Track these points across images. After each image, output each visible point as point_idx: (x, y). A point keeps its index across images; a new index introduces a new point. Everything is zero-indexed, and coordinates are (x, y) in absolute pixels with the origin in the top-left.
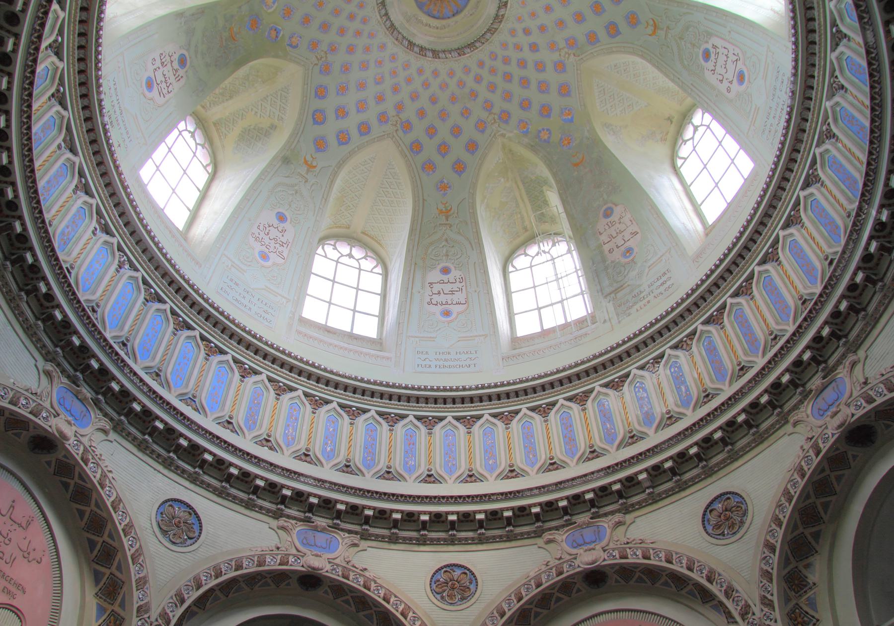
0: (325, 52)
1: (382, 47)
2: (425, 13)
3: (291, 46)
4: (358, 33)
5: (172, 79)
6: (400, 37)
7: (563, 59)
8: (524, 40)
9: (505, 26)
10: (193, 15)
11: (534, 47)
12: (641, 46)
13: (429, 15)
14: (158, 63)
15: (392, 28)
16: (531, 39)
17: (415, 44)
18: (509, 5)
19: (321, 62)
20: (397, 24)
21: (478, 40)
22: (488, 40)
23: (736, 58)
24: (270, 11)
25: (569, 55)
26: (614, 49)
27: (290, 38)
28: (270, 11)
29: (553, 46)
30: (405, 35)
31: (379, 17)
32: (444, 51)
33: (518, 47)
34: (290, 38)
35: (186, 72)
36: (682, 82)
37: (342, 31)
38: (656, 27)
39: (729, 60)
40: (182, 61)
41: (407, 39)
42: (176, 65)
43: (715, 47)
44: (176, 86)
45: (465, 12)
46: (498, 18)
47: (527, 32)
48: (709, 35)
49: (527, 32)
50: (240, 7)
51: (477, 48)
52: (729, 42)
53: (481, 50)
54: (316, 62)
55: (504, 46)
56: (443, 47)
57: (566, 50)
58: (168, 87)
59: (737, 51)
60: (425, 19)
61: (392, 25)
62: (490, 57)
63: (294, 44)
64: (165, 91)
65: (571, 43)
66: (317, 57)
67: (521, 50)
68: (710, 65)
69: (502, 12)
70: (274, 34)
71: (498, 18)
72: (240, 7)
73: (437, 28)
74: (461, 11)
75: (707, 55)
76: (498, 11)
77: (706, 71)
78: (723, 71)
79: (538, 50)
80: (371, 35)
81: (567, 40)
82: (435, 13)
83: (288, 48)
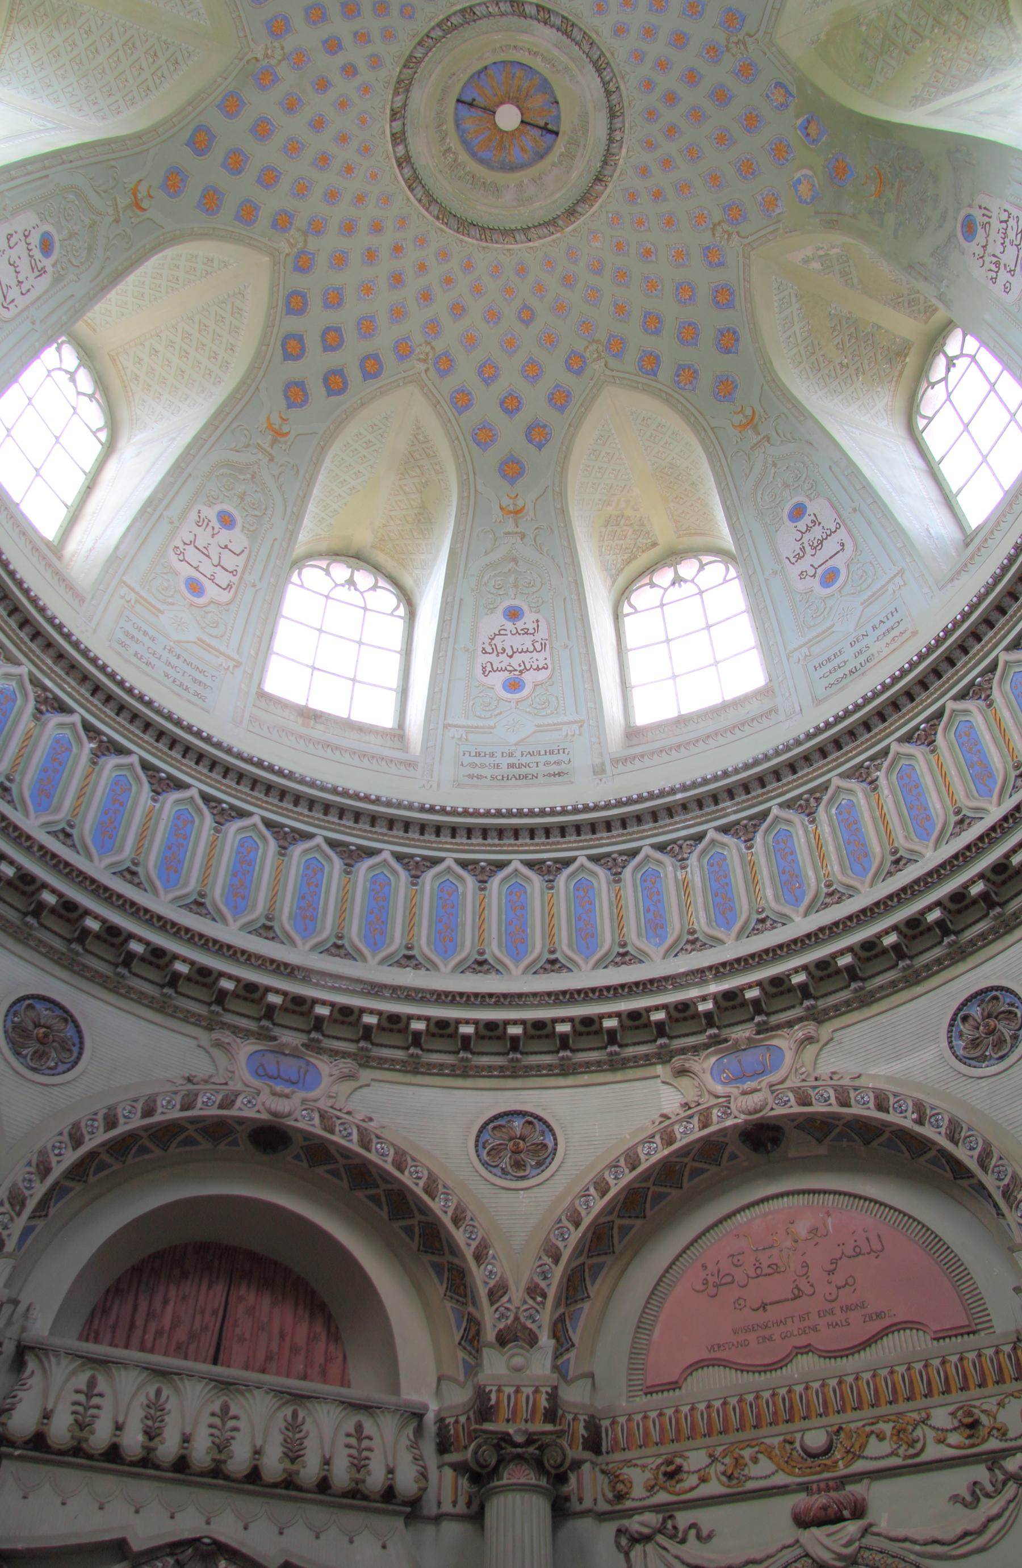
0: (728, 50)
1: (620, 31)
2: (537, 73)
3: (787, 92)
4: (663, 65)
5: (995, 225)
6: (586, 48)
7: (276, 44)
8: (354, 54)
9: (392, 70)
10: (926, 279)
11: (333, 46)
12: (148, 150)
13: (531, 68)
14: (1003, 276)
15: (600, 65)
16: (340, 59)
17: (558, 30)
18: (388, 112)
19: (740, 37)
20: (590, 67)
21: (437, 41)
22: (420, 44)
23: (9, 300)
24: (809, 173)
25: (266, 56)
26: (190, 109)
27: (784, 106)
28: (809, 173)
29: (299, 59)
30: (577, 48)
31: (622, 87)
32: (502, 15)
33: (362, 38)
34: (787, 106)
35: (970, 206)
36: (63, 163)
37: (692, 78)
38: (137, 205)
39: (14, 283)
40: (969, 228)
41: (573, 40)
42: (980, 236)
43: (43, 271)
44: (994, 205)
45: (464, 78)
46: (403, 86)
47: (350, 70)
48: (57, 279)
49: (350, 70)
50: (854, 216)
51: (439, 25)
52: (27, 307)
53: (431, 19)
54: (747, 39)
55: (388, 35)
56: (504, 21)
57: (273, 62)
58: (1006, 222)
59: (13, 311)
60: (537, 64)
61: (599, 71)
62: (413, 8)
63: (782, 91)
64: (1012, 223)
65: (266, 78)
66: (746, 48)
67: (356, 34)
68: (35, 239)
69: (399, 100)
70: (813, 130)
71: (403, 86)
72: (854, 216)
73: (515, 47)
74: (472, 77)
75: (47, 246)
76: (407, 98)
77: (38, 222)
78: (13, 254)
79: (325, 42)
80: (639, 56)
81: (276, 79)
82: (519, 73)
83: (794, 91)
